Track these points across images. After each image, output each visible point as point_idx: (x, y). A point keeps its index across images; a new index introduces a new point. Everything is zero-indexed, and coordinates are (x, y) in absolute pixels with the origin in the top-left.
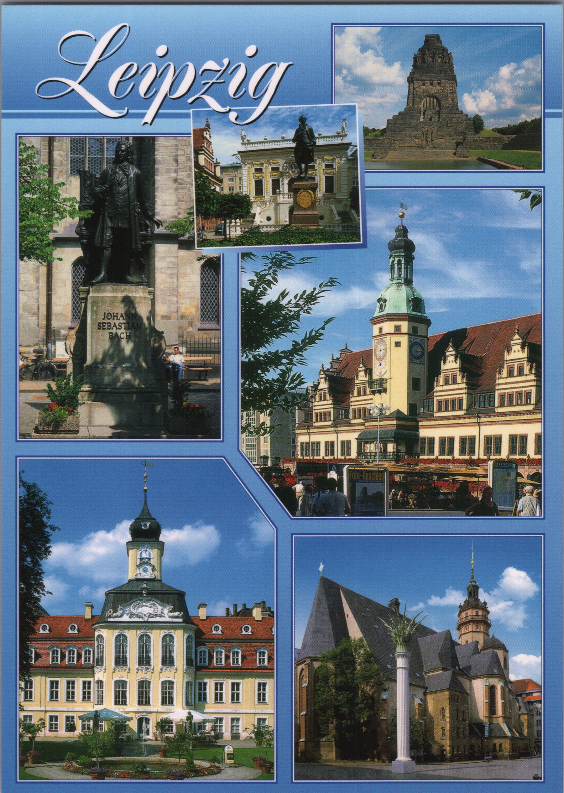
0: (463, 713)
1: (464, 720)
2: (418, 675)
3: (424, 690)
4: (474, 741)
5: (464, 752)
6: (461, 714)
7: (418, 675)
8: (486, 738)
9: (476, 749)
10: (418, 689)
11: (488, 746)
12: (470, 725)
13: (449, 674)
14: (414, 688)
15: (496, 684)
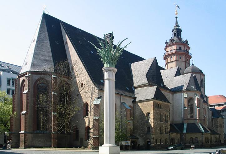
0: (166, 116)
1: (166, 121)
2: (128, 89)
3: (132, 100)
4: (174, 135)
5: (166, 143)
6: (164, 117)
7: (128, 89)
8: (184, 134)
9: (176, 141)
10: (128, 98)
11: (185, 139)
12: (171, 125)
13: (154, 89)
14: (124, 97)
15: (193, 97)
